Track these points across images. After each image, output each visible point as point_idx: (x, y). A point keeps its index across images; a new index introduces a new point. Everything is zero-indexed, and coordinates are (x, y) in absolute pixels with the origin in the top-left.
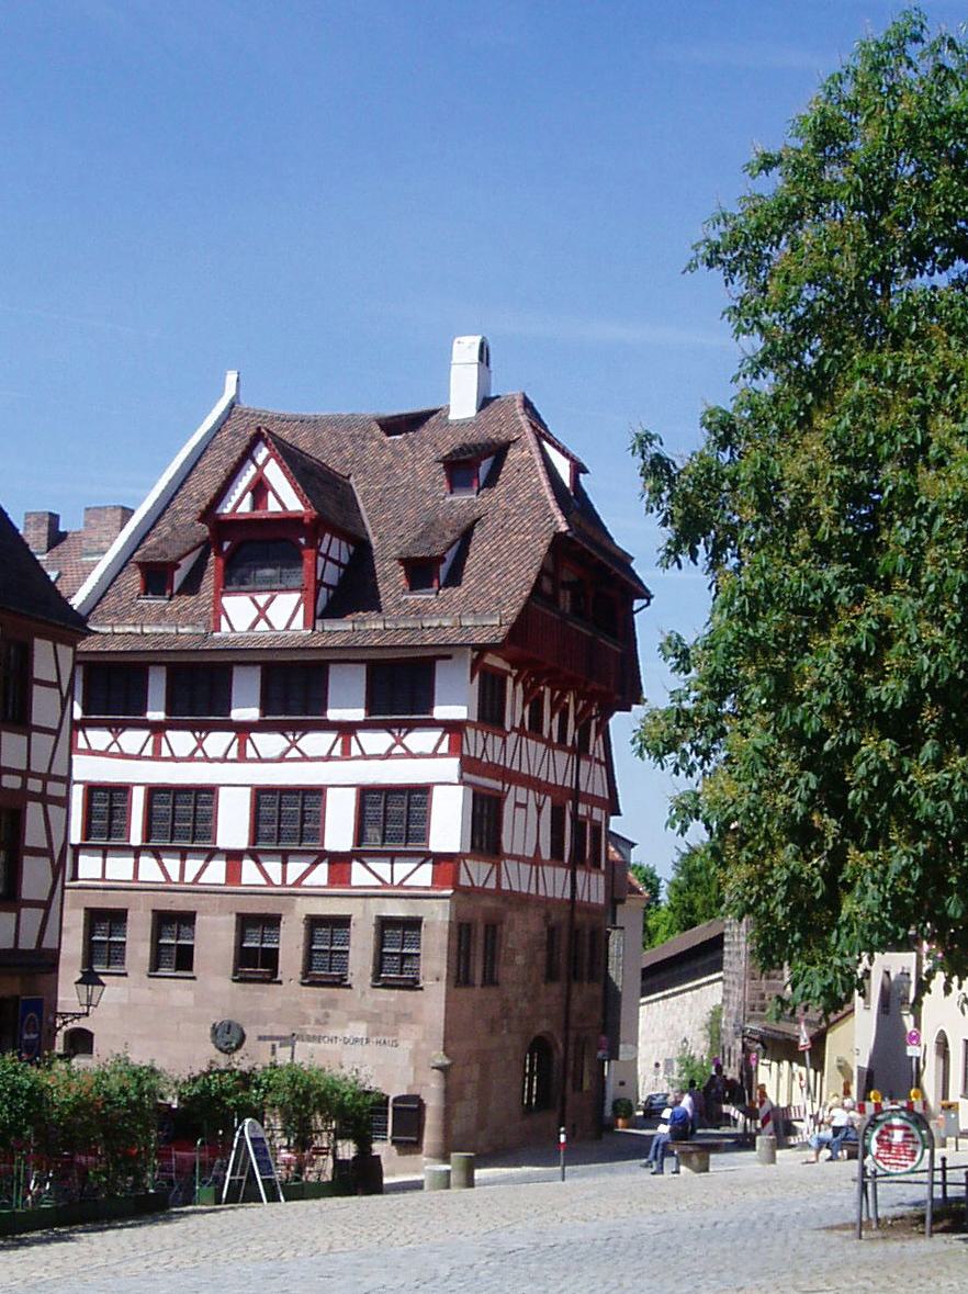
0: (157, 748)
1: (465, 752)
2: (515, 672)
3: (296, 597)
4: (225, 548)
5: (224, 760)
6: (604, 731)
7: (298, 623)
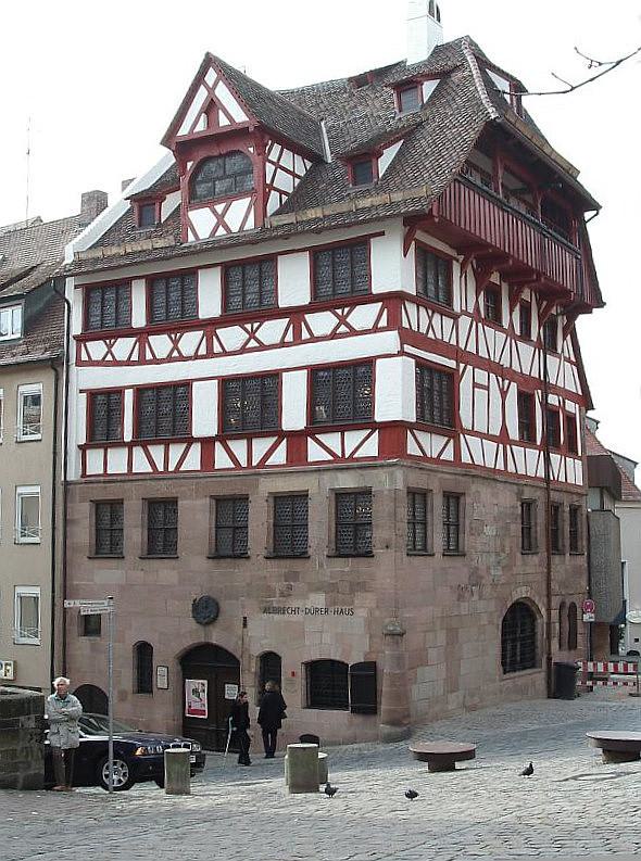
0: (142, 353)
2: (461, 258)
3: (246, 202)
4: (189, 167)
5: (196, 357)
6: (570, 331)
7: (250, 224)
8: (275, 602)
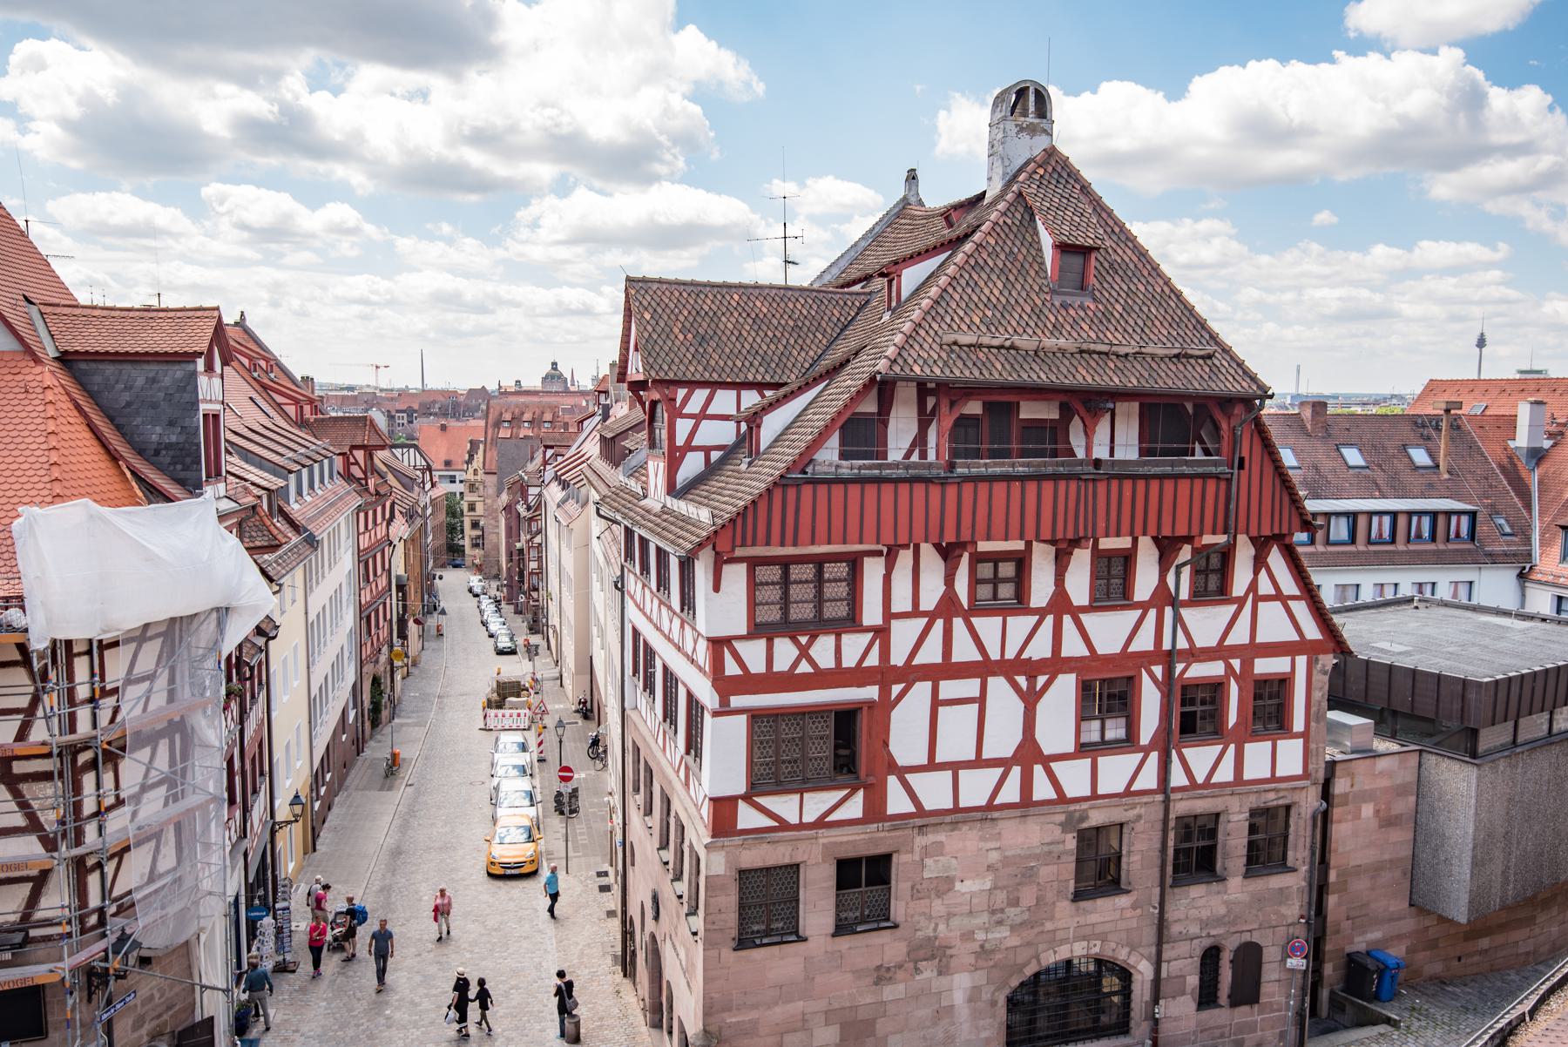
1: (731, 669)
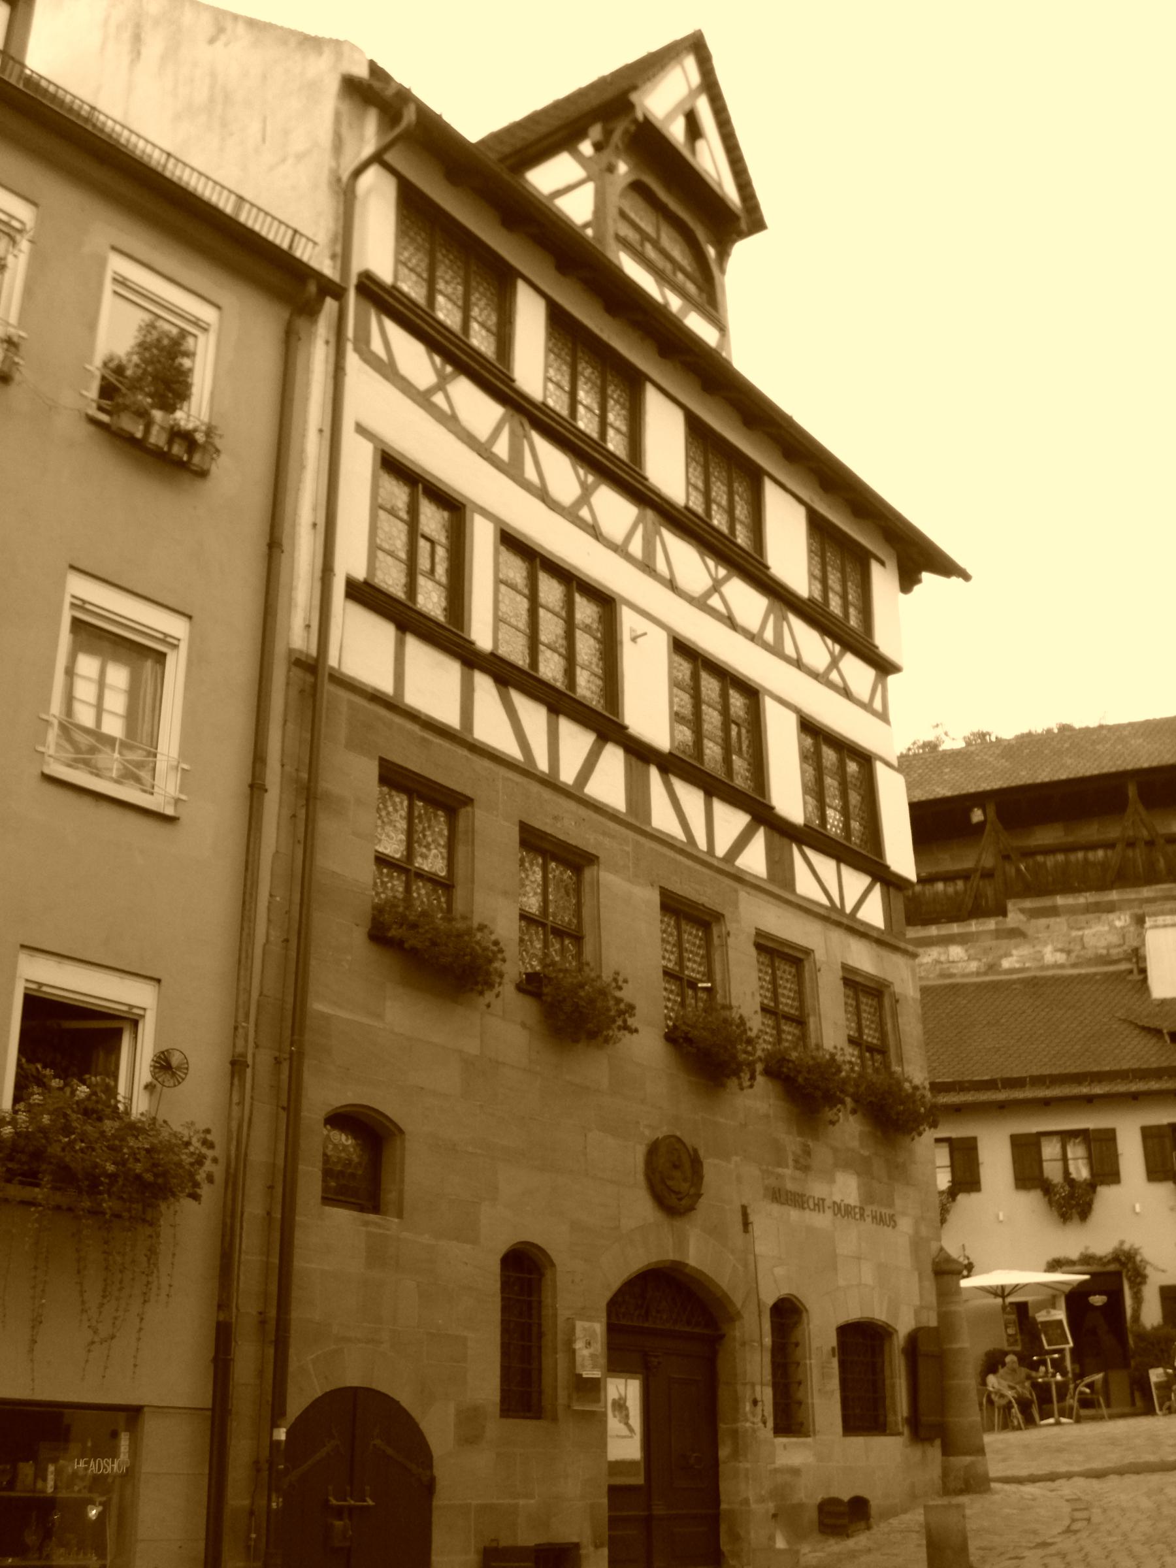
8: (789, 1177)
